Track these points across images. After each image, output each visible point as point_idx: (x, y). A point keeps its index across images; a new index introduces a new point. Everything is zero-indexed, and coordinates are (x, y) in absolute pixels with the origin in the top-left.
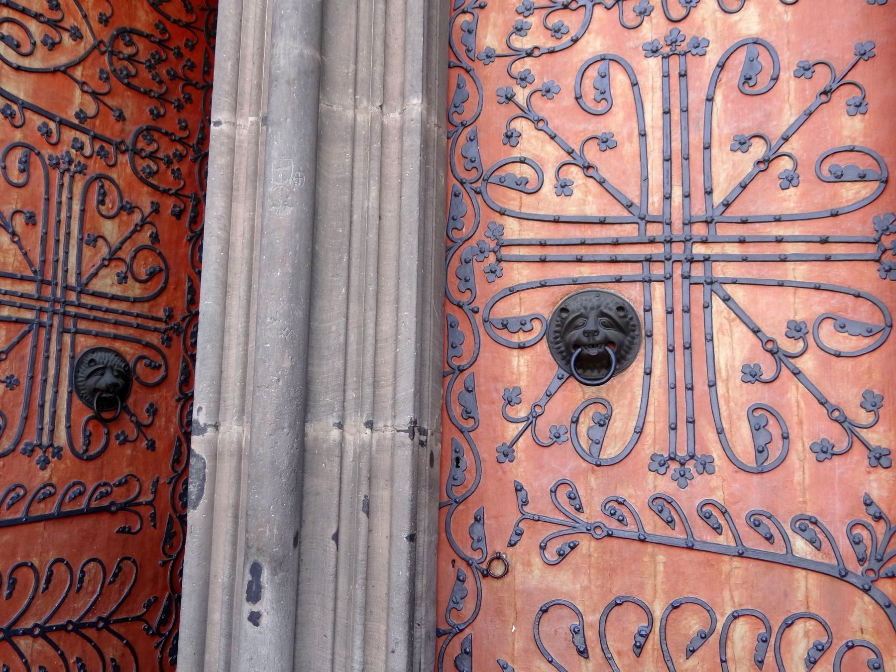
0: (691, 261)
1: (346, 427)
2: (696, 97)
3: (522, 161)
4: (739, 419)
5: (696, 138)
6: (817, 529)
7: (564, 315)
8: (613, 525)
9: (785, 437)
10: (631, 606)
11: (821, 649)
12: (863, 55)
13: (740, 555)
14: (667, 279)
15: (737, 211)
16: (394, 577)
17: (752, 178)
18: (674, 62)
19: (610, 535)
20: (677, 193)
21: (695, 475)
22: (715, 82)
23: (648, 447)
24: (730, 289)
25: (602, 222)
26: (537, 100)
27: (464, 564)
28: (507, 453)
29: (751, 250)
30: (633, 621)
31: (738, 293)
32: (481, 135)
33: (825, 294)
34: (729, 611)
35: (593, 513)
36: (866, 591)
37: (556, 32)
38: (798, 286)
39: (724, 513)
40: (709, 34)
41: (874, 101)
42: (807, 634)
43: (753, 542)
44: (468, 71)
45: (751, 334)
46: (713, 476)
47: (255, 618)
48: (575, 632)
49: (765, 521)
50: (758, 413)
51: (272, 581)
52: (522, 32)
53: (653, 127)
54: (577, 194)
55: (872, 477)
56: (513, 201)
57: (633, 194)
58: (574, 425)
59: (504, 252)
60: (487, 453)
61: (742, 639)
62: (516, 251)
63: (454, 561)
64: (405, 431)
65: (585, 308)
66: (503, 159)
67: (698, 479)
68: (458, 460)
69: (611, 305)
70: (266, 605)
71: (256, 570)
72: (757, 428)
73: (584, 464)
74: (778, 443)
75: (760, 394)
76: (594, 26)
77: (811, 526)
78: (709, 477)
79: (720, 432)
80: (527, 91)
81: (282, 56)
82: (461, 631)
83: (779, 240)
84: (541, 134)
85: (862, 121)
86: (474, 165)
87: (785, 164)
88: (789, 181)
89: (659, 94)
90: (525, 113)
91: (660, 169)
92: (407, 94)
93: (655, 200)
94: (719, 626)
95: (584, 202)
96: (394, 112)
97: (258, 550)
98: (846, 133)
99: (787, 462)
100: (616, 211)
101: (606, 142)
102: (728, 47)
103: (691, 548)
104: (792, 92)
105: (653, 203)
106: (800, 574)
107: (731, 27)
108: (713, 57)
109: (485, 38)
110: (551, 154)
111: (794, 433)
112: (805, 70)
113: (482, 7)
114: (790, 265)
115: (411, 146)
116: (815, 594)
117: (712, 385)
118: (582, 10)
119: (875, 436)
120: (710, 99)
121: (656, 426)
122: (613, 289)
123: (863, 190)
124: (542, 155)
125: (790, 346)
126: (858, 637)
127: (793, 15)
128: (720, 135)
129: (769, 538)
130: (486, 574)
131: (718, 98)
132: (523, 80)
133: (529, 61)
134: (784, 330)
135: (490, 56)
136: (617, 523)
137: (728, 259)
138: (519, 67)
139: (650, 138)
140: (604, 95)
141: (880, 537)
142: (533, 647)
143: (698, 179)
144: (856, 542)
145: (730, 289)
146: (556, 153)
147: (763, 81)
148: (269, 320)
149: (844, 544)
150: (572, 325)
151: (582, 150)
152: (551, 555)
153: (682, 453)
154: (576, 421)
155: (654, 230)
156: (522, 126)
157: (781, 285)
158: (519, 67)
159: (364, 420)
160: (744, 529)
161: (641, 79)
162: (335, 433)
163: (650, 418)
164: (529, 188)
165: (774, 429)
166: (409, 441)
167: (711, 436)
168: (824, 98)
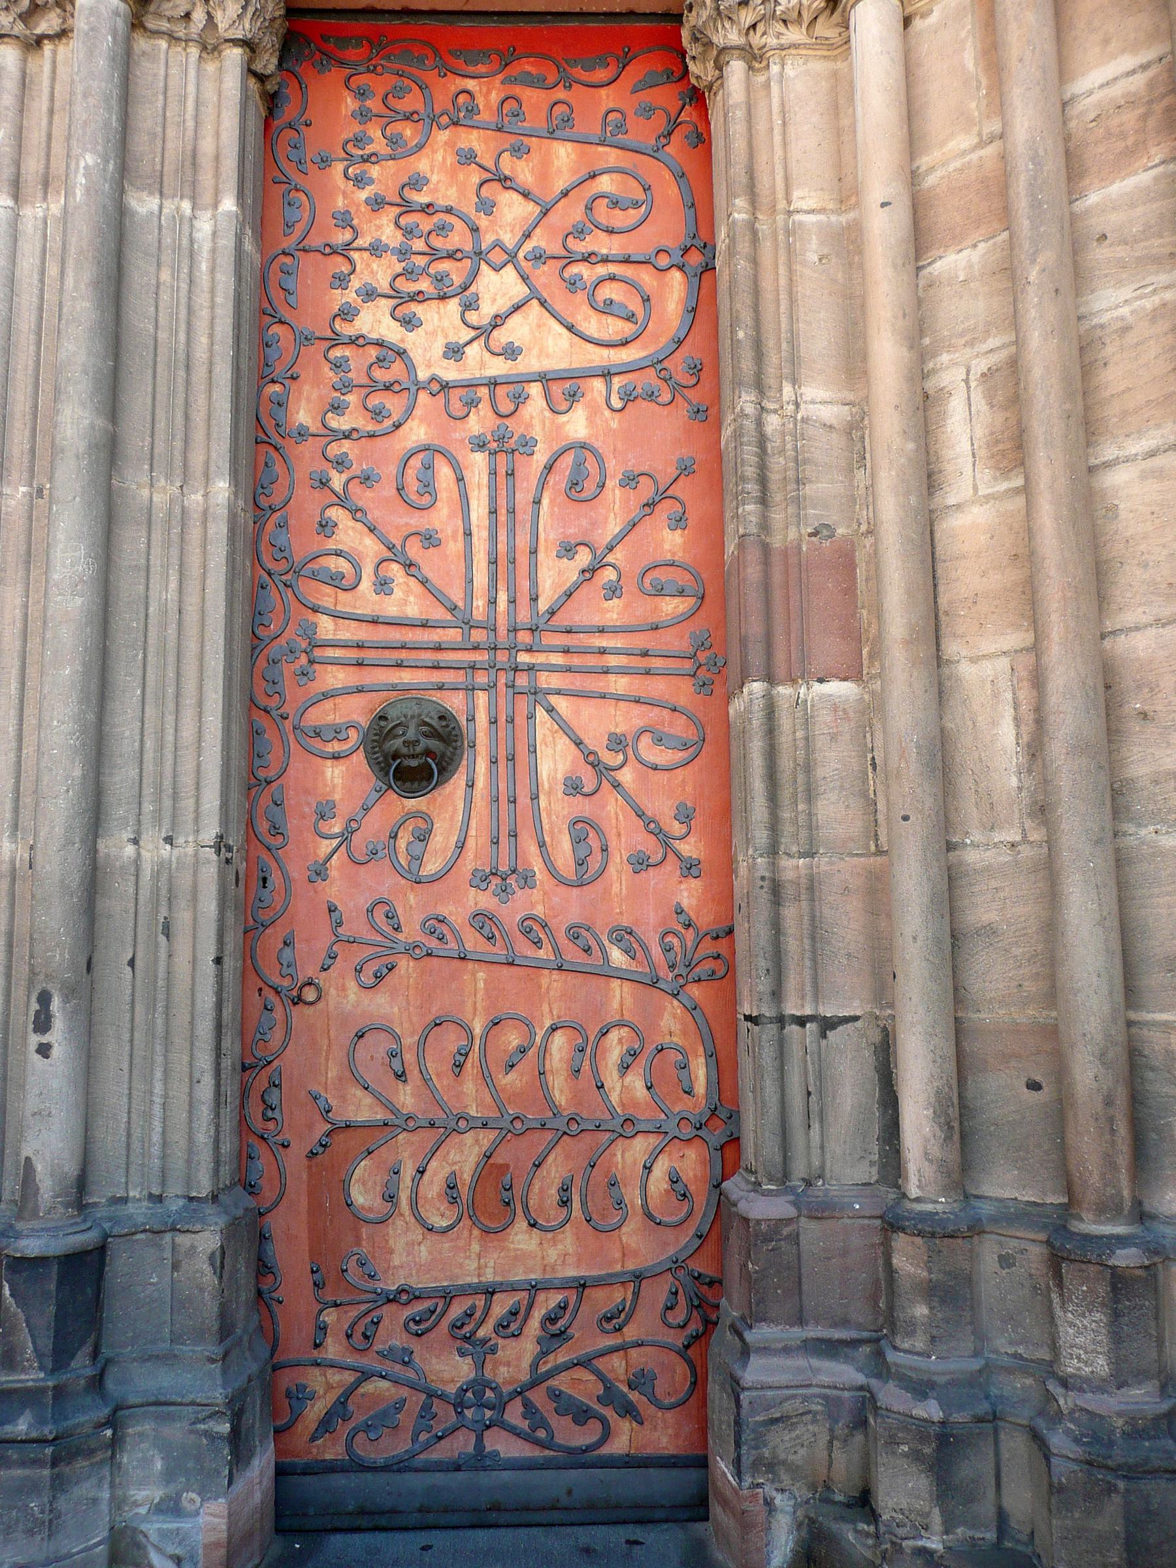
0: (516, 670)
1: (142, 843)
2: (523, 498)
3: (338, 554)
4: (560, 832)
5: (523, 541)
6: (632, 939)
7: (383, 723)
8: (433, 943)
9: (605, 849)
10: (452, 1026)
11: (634, 1054)
12: (685, 470)
13: (560, 969)
14: (491, 687)
15: (560, 620)
16: (199, 1004)
17: (577, 586)
18: (502, 459)
19: (429, 955)
20: (502, 598)
21: (517, 889)
22: (543, 484)
23: (469, 862)
24: (554, 700)
25: (425, 625)
26: (354, 487)
27: (273, 993)
28: (320, 872)
29: (576, 661)
30: (451, 1040)
31: (562, 704)
32: (292, 522)
33: (644, 708)
34: (548, 1023)
35: (411, 932)
36: (675, 996)
37: (377, 414)
38: (618, 699)
39: (544, 926)
40: (537, 433)
41: (693, 517)
42: (620, 1041)
43: (572, 954)
44: (277, 449)
45: (573, 746)
46: (535, 891)
47: (44, 1050)
48: (393, 1055)
49: (584, 933)
50: (579, 826)
51: (64, 1009)
52: (339, 411)
53: (478, 526)
54: (398, 593)
55: (683, 887)
56: (326, 597)
57: (456, 595)
58: (392, 841)
59: (318, 653)
60: (297, 872)
61: (560, 1049)
62: (330, 653)
63: (260, 990)
64: (210, 847)
65: (405, 716)
66: (315, 549)
67: (519, 893)
68: (265, 880)
69: (432, 714)
70: (57, 1036)
71: (45, 999)
72: (578, 841)
73: (403, 882)
74: (598, 856)
75: (582, 807)
76: (418, 412)
77: (627, 937)
78: (530, 891)
79: (542, 845)
80: (344, 477)
81: (69, 426)
82: (270, 1063)
83: (603, 652)
84: (359, 525)
85: (682, 536)
86: (283, 554)
87: (609, 575)
88: (613, 591)
89: (485, 492)
90: (342, 501)
91: (485, 571)
92: (212, 476)
93: (480, 603)
94: (538, 1039)
95: (405, 602)
96: (195, 493)
97: (47, 976)
98: (667, 546)
99: (605, 874)
100: (438, 614)
101: (430, 540)
102: (556, 449)
103: (511, 964)
104: (617, 501)
105: (478, 607)
106: (615, 984)
107: (559, 428)
108: (541, 457)
109: (298, 413)
110: (370, 548)
111: (613, 844)
112: (630, 480)
113: (293, 378)
114: (612, 678)
115: (217, 533)
116: (629, 1002)
117: (535, 797)
118: (406, 393)
119: (687, 847)
120: (537, 502)
122: (436, 696)
124: (360, 548)
125: (611, 759)
126: (667, 1039)
127: (619, 422)
128: (546, 540)
129: (587, 950)
130: (298, 1001)
131: (545, 502)
132: (340, 463)
133: (346, 445)
134: (605, 742)
135: (303, 433)
136: (437, 941)
137: (552, 669)
138: (334, 450)
139: (475, 539)
140: (428, 486)
141: (689, 944)
142: (348, 1074)
143: (524, 585)
144: (669, 949)
145: (554, 700)
146: (376, 548)
147: (590, 488)
148: (55, 723)
149: (656, 951)
150: (390, 734)
151: (403, 546)
152: (367, 978)
153: (504, 869)
154: (395, 837)
155: (478, 636)
156: (335, 513)
157: (603, 696)
158: (334, 450)
159: (164, 835)
160: (563, 941)
161: (467, 475)
162: (130, 850)
163: (472, 832)
164: (345, 583)
165: (594, 841)
166: (215, 857)
167: (533, 849)
168: (647, 510)
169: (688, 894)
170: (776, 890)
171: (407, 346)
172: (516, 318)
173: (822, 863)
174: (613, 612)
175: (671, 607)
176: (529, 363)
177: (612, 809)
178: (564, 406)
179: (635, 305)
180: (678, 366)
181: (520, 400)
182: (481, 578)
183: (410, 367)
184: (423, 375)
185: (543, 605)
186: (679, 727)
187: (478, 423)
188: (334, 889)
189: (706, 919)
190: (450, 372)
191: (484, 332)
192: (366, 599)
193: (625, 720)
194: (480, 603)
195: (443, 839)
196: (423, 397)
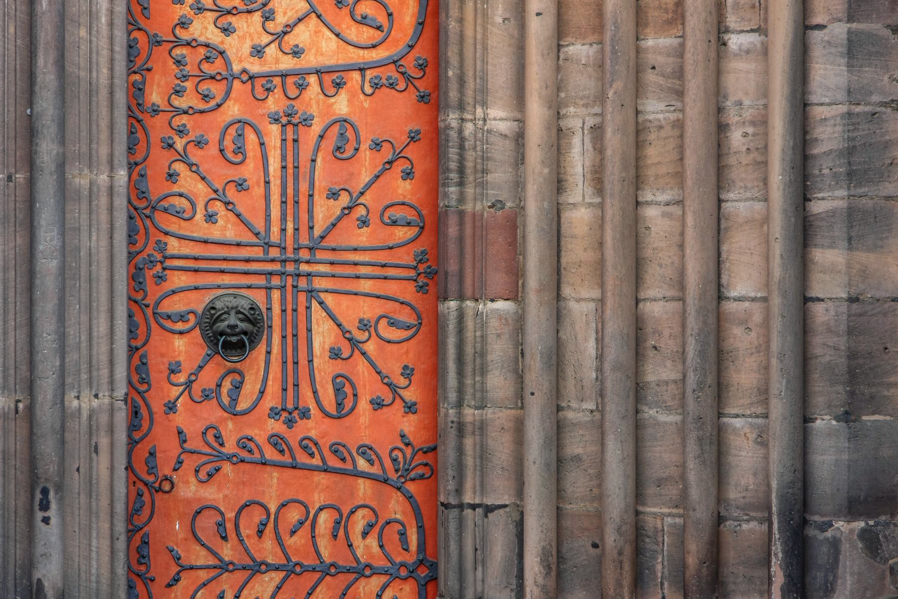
0: (298, 275)
1: (81, 398)
2: (305, 155)
3: (181, 195)
4: (327, 383)
5: (304, 186)
6: (372, 453)
7: (213, 312)
8: (244, 455)
9: (355, 395)
10: (257, 507)
11: (371, 526)
12: (413, 138)
13: (325, 471)
14: (282, 288)
16: (116, 494)
17: (339, 219)
19: (242, 461)
20: (290, 226)
21: (298, 420)
22: (317, 149)
24: (323, 296)
25: (238, 245)
27: (142, 484)
28: (171, 407)
29: (338, 270)
30: (258, 516)
31: (329, 299)
32: (149, 172)
33: (383, 301)
34: (317, 506)
36: (399, 489)
37: (205, 97)
39: (316, 444)
40: (314, 110)
41: (418, 173)
42: (363, 517)
43: (333, 462)
44: (139, 121)
45: (336, 327)
46: (310, 421)
47: (46, 520)
48: (219, 525)
49: (341, 448)
50: (339, 380)
51: (56, 498)
52: (180, 94)
53: (274, 176)
54: (221, 222)
55: (405, 419)
56: (174, 225)
58: (218, 388)
59: (168, 263)
60: (157, 406)
61: (325, 522)
63: (134, 482)
64: (122, 400)
65: (228, 307)
66: (167, 192)
67: (300, 422)
68: (136, 413)
69: (245, 306)
70: (53, 512)
71: (45, 492)
72: (338, 390)
73: (225, 415)
74: (350, 397)
75: (339, 367)
77: (368, 451)
78: (307, 421)
79: (315, 392)
80: (184, 141)
81: (45, 155)
82: (141, 529)
83: (356, 264)
84: (194, 175)
85: (410, 184)
86: (144, 195)
87: (361, 211)
88: (364, 222)
89: (279, 152)
90: (183, 158)
91: (279, 207)
92: (116, 166)
93: (275, 229)
94: (311, 516)
95: (225, 228)
96: (102, 174)
97: (46, 479)
98: (400, 191)
99: (356, 411)
100: (250, 238)
101: (241, 185)
102: (327, 122)
103: (294, 467)
104: (368, 160)
105: (274, 232)
106: (361, 481)
108: (317, 128)
109: (151, 94)
110: (200, 190)
111: (360, 391)
112: (377, 146)
113: (149, 70)
114: (362, 281)
115: (120, 205)
116: (369, 492)
117: (310, 361)
118: (225, 82)
119: (408, 394)
120: (314, 161)
121: (273, 387)
123: (411, 233)
124: (195, 190)
125: (361, 336)
126: (393, 516)
127: (370, 103)
128: (319, 186)
129: (343, 460)
130: (160, 490)
131: (319, 160)
132: (181, 132)
133: (185, 119)
134: (357, 324)
135: (156, 111)
136: (247, 453)
138: (178, 121)
139: (272, 185)
140: (240, 150)
141: (409, 456)
142: (191, 536)
143: (304, 216)
144: (394, 460)
145: (323, 296)
146: (205, 190)
148: (45, 335)
149: (388, 463)
150: (218, 319)
151: (224, 190)
152: (202, 475)
153: (290, 406)
154: (219, 386)
155: (274, 253)
156: (179, 167)
157: (356, 294)
158: (178, 121)
159: (94, 393)
160: (327, 454)
161: (266, 140)
162: (75, 403)
163: (270, 383)
164: (186, 216)
165: (348, 389)
166: (124, 407)
167: (310, 394)
168: (387, 166)
169: (409, 425)
170: (461, 429)
171: (225, 47)
172: (301, 27)
173: (489, 413)
174: (363, 237)
175: (402, 234)
176: (310, 60)
177: (361, 370)
178: (332, 91)
179: (382, 19)
180: (409, 65)
181: (302, 87)
182: (275, 212)
183: (228, 64)
184: (236, 68)
185: (317, 232)
186: (405, 316)
187: (275, 103)
188: (180, 419)
189: (419, 439)
190: (255, 68)
191: (279, 37)
192: (199, 227)
193: (368, 309)
194: (275, 229)
195: (251, 388)
196: (237, 84)
